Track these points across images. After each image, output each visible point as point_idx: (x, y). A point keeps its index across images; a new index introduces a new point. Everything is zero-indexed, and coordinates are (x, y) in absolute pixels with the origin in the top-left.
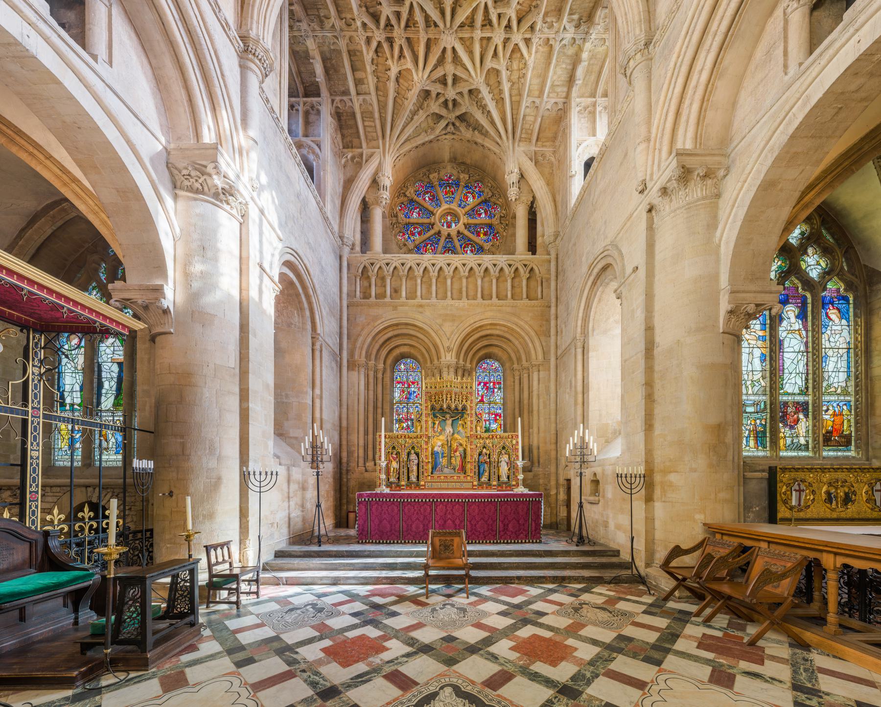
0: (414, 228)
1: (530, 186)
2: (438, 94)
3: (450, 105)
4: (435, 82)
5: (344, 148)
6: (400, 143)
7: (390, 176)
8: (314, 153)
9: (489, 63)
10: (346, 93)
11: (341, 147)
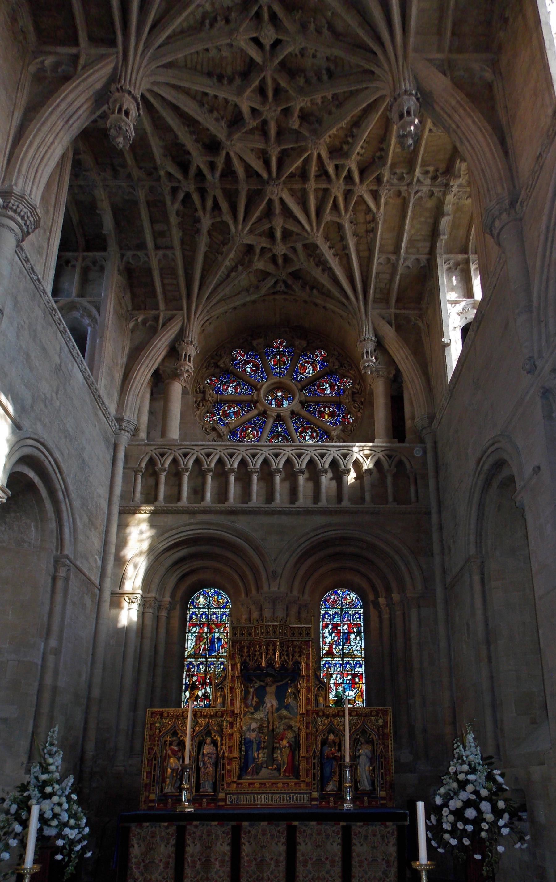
0: (229, 408)
1: (389, 355)
2: (263, 249)
3: (280, 261)
4: (260, 235)
5: (134, 309)
6: (211, 304)
7: (196, 343)
8: (90, 316)
9: (328, 217)
10: (142, 246)
11: (130, 308)
